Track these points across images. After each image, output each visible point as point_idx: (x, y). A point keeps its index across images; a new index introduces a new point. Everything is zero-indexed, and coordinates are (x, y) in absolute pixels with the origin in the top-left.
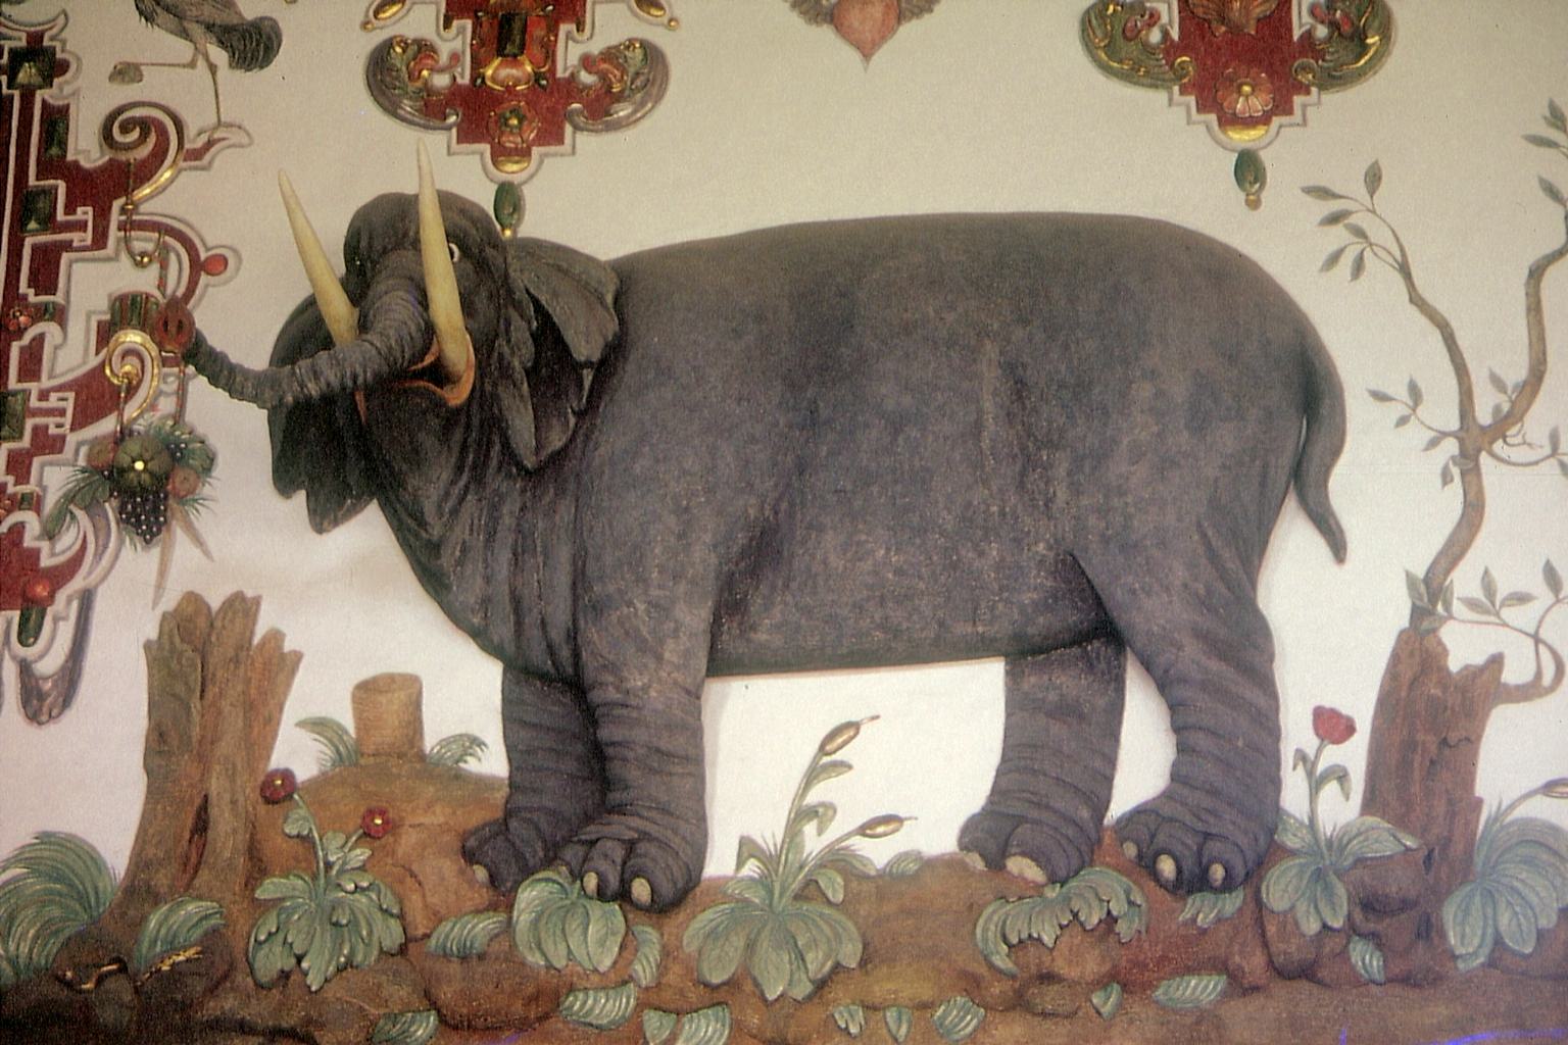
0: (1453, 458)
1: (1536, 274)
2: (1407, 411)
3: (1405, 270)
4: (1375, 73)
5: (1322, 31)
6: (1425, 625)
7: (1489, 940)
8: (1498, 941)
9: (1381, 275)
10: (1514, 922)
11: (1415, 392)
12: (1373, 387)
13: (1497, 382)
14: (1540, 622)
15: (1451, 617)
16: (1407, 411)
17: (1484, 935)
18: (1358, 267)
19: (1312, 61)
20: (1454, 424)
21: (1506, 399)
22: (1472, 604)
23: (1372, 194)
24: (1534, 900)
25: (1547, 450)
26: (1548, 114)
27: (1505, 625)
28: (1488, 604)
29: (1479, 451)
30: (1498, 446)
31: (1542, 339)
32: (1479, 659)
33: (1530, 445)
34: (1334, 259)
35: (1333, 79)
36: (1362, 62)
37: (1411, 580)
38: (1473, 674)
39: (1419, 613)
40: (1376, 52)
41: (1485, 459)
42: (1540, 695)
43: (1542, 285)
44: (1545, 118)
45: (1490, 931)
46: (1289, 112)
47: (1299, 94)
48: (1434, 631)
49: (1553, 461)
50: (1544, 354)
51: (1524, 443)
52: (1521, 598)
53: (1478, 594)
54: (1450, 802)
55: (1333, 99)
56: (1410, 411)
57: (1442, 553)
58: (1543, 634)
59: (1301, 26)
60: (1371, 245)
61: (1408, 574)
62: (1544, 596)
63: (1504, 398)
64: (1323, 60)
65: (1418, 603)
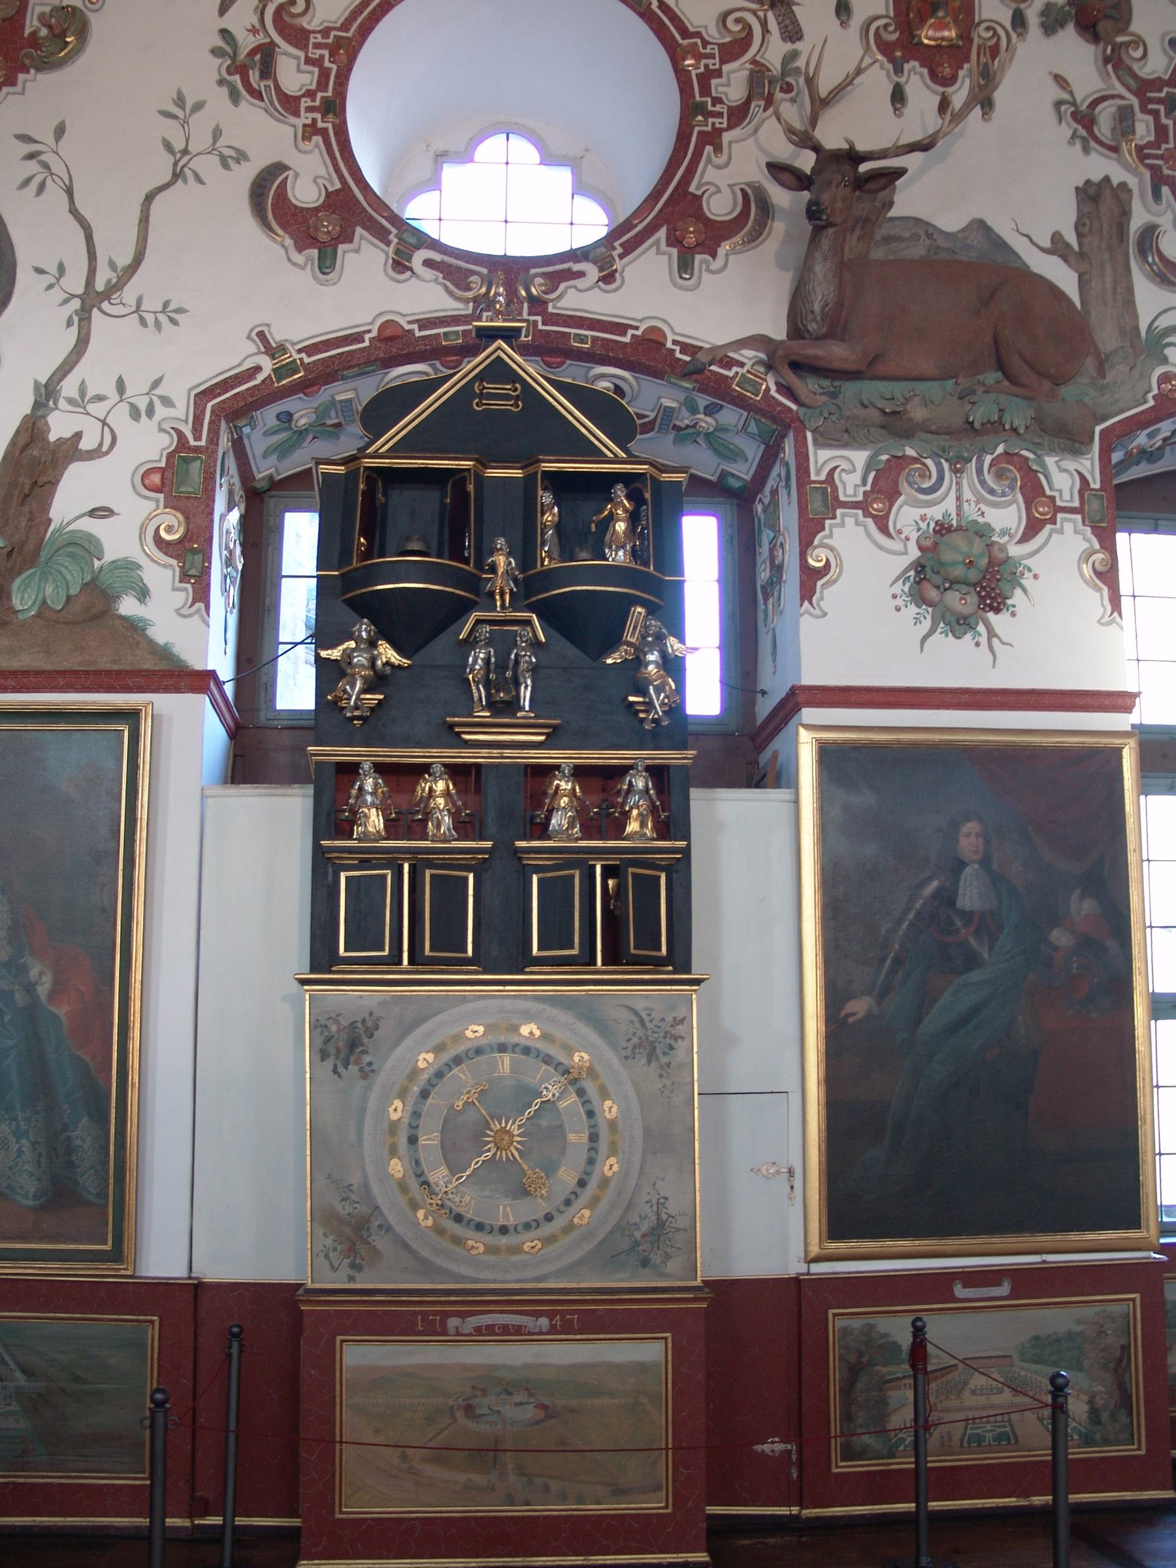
0: (76, 311)
1: (149, 198)
2: (54, 281)
3: (70, 192)
4: (73, 62)
5: (44, 32)
6: (40, 413)
7: (39, 602)
8: (44, 602)
9: (55, 195)
10: (55, 591)
11: (61, 269)
12: (36, 265)
13: (112, 265)
14: (108, 413)
15: (57, 408)
16: (54, 281)
17: (36, 599)
18: (42, 188)
19: (33, 51)
20: (80, 290)
21: (115, 275)
22: (71, 401)
23: (57, 140)
24: (69, 577)
25: (134, 309)
26: (175, 98)
27: (88, 414)
28: (80, 402)
29: (93, 306)
30: (105, 305)
31: (145, 239)
32: (67, 434)
33: (123, 304)
34: (27, 182)
35: (46, 65)
36: (63, 54)
37: (37, 384)
38: (61, 442)
39: (37, 405)
40: (72, 50)
41: (95, 312)
42: (99, 457)
43: (152, 207)
44: (173, 100)
45: (40, 596)
46: (14, 84)
47: (22, 72)
48: (44, 417)
49: (136, 315)
50: (145, 248)
51: (121, 303)
52: (100, 398)
53: (75, 395)
54: (31, 520)
55: (44, 78)
56: (55, 281)
57: (59, 369)
58: (107, 421)
59: (31, 27)
60: (52, 174)
61: (36, 381)
62: (114, 396)
63: (115, 275)
64: (42, 51)
65: (39, 399)
